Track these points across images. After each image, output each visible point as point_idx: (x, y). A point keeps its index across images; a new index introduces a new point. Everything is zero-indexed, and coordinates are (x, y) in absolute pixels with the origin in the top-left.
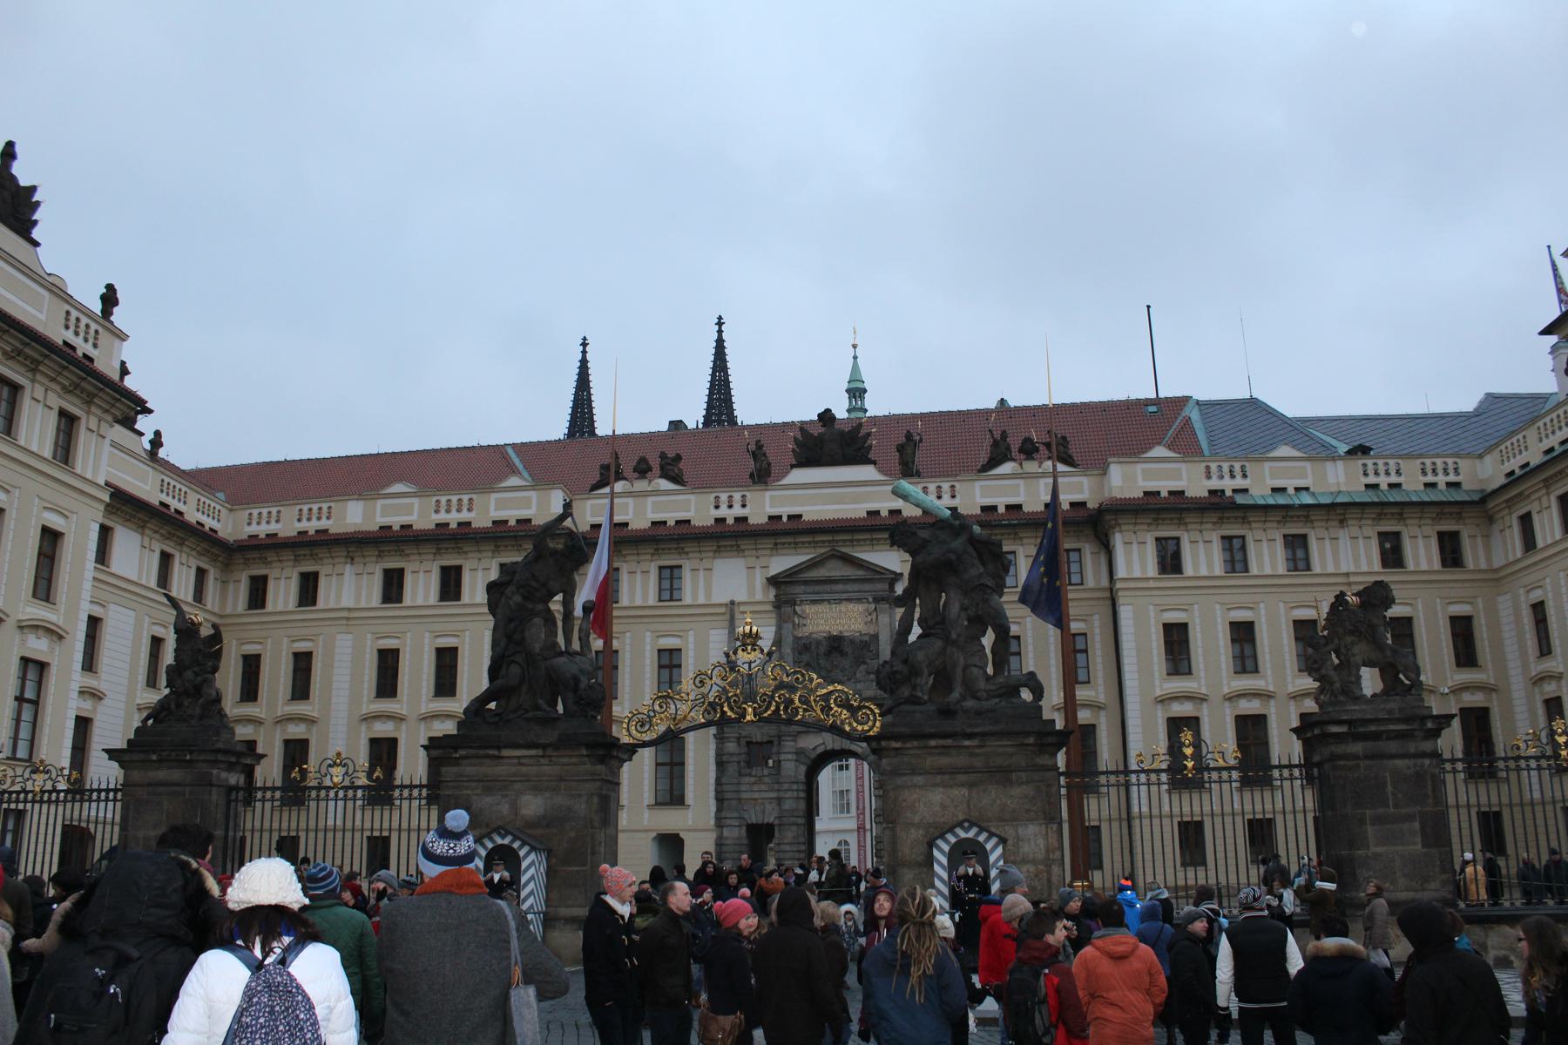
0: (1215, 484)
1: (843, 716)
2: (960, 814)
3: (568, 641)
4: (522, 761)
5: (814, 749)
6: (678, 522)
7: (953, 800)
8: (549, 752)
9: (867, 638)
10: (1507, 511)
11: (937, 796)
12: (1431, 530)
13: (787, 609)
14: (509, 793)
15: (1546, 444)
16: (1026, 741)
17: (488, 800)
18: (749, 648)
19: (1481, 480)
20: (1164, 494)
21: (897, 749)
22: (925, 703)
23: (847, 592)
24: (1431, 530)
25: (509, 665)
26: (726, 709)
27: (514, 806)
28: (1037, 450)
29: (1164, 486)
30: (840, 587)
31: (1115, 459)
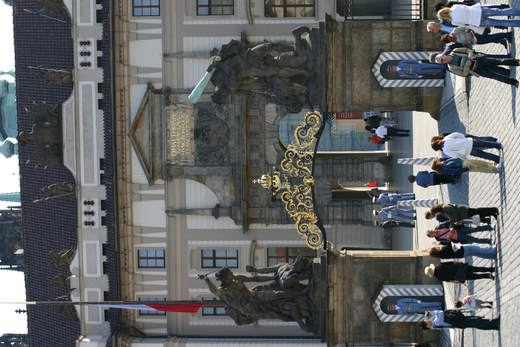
2: (366, 72)
3: (269, 279)
5: (277, 151)
6: (104, 254)
7: (359, 76)
9: (197, 111)
11: (357, 84)
13: (173, 170)
14: (352, 305)
16: (330, 37)
17: (356, 317)
18: (274, 181)
21: (333, 104)
22: (309, 89)
23: (161, 126)
26: (306, 193)
27: (359, 303)
30: (157, 131)
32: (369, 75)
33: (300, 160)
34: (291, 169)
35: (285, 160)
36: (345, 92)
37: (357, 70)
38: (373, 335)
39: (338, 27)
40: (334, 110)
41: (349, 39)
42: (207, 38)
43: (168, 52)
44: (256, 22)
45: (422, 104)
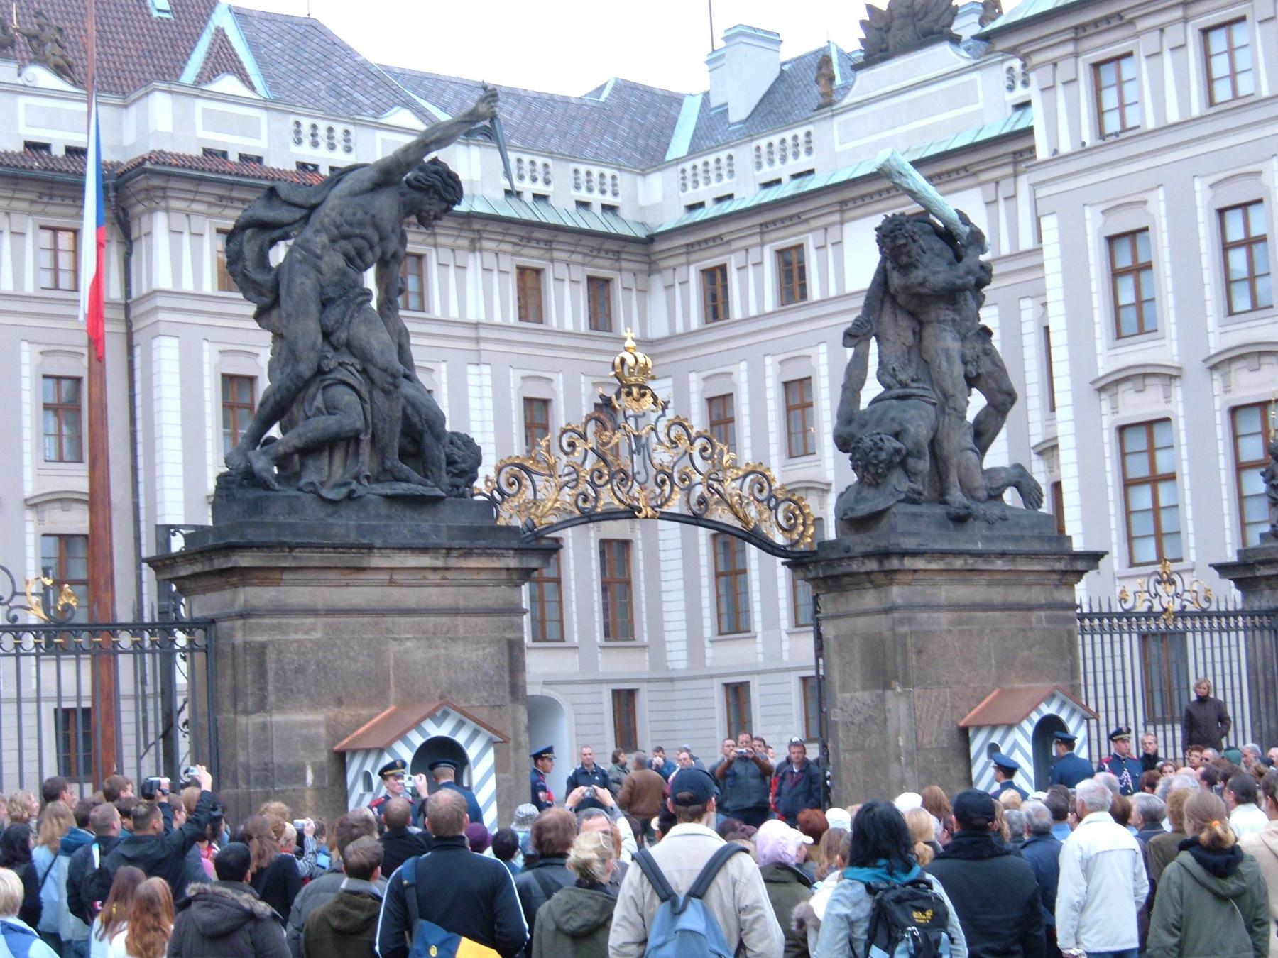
0: (306, 153)
4: (396, 577)
8: (453, 562)
10: (683, 259)
12: (581, 274)
15: (768, 173)
19: (642, 208)
20: (234, 157)
24: (581, 274)
25: (325, 388)
28: (12, 43)
29: (235, 144)
31: (164, 86)
38: (277, 718)
40: (899, 577)
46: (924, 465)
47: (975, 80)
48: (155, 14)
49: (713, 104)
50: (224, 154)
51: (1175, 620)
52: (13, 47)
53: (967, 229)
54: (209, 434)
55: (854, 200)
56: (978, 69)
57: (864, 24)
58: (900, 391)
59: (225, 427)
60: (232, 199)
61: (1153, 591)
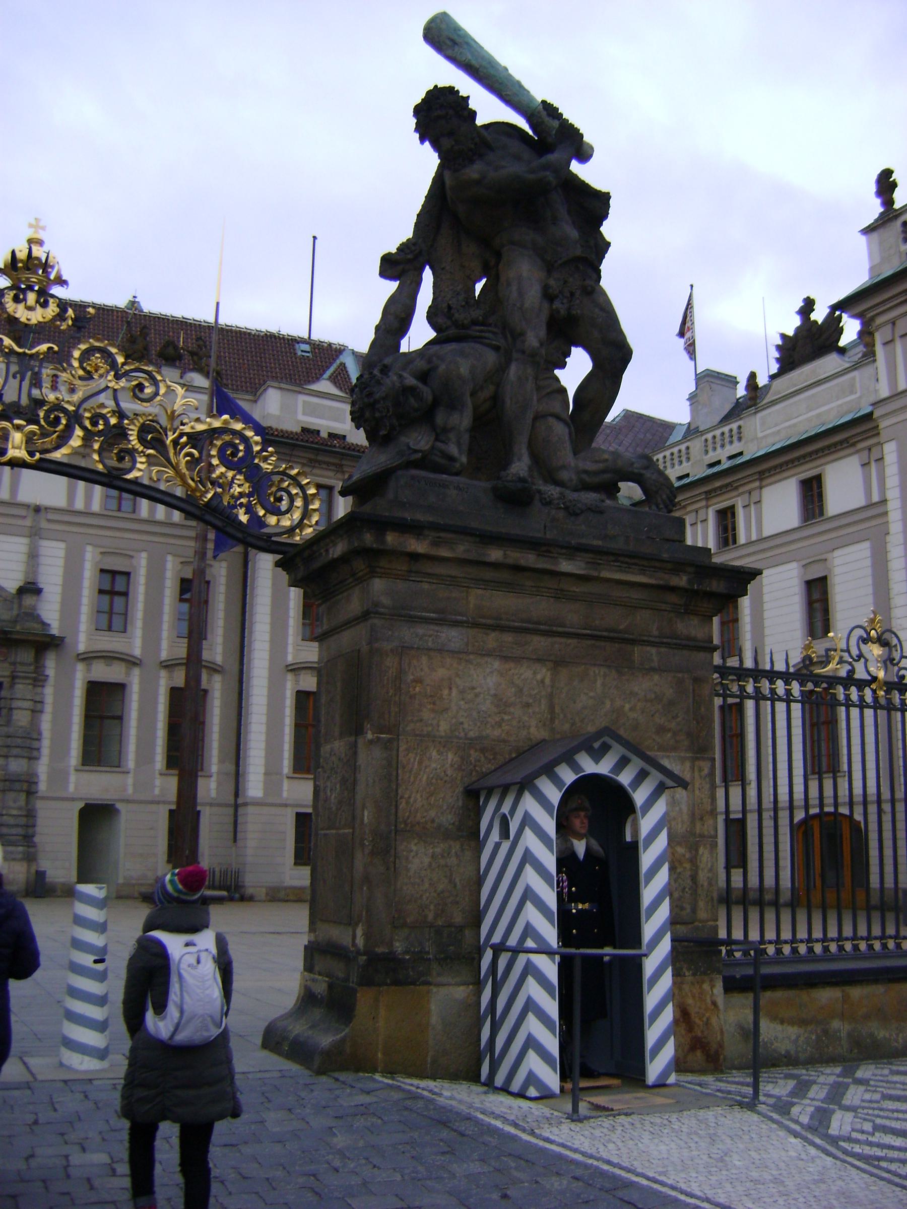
1: (236, 490)
2: (533, 723)
7: (520, 691)
18: (31, 297)
21: (414, 557)
22: (457, 474)
31: (276, 384)
32: (525, 733)
33: (113, 421)
34: (80, 378)
35: (120, 359)
36: (456, 624)
37: (542, 681)
39: (695, 621)
41: (655, 658)
42: (59, 580)
43: (43, 513)
44: (80, 667)
45: (396, 983)
46: (463, 420)
47: (854, 378)
48: (299, 353)
49: (692, 428)
50: (319, 431)
51: (887, 692)
52: (180, 360)
53: (556, 124)
54: (291, 622)
55: (769, 470)
56: (856, 369)
57: (778, 348)
58: (452, 331)
59: (304, 618)
60: (320, 462)
61: (855, 652)
